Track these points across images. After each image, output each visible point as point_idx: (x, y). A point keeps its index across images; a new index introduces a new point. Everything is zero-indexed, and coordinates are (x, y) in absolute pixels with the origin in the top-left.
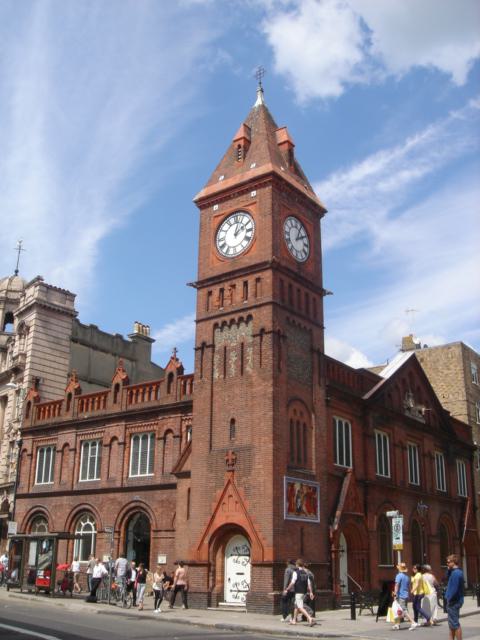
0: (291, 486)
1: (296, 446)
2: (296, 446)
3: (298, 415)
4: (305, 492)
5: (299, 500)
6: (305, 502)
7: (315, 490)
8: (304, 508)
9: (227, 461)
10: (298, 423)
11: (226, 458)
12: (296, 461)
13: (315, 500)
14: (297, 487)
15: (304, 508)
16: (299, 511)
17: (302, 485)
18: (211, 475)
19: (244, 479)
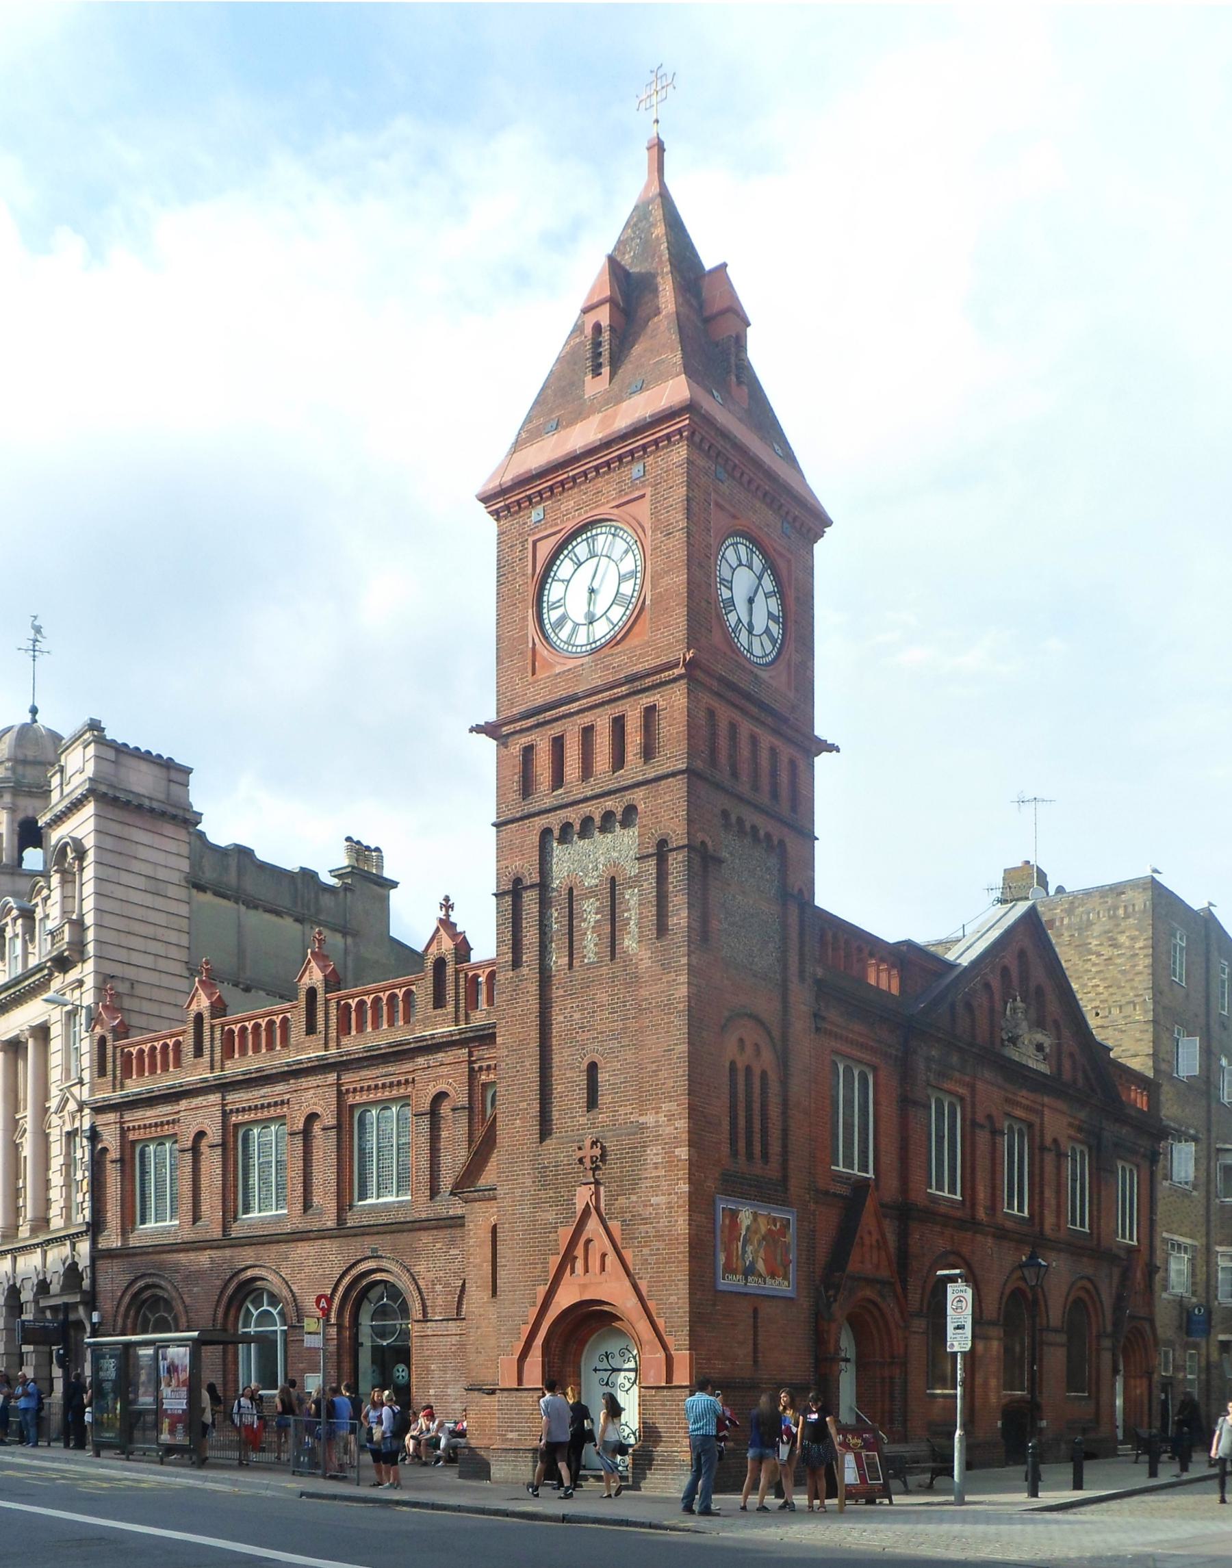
0: (734, 1214)
1: (742, 1122)
2: (742, 1122)
3: (749, 1050)
4: (763, 1230)
5: (749, 1249)
6: (762, 1253)
7: (786, 1224)
8: (761, 1266)
9: (581, 1161)
10: (748, 1069)
11: (580, 1154)
12: (742, 1159)
13: (786, 1247)
14: (745, 1218)
15: (761, 1266)
16: (749, 1271)
17: (755, 1215)
18: (542, 1195)
19: (622, 1201)
